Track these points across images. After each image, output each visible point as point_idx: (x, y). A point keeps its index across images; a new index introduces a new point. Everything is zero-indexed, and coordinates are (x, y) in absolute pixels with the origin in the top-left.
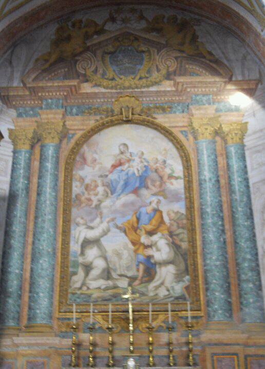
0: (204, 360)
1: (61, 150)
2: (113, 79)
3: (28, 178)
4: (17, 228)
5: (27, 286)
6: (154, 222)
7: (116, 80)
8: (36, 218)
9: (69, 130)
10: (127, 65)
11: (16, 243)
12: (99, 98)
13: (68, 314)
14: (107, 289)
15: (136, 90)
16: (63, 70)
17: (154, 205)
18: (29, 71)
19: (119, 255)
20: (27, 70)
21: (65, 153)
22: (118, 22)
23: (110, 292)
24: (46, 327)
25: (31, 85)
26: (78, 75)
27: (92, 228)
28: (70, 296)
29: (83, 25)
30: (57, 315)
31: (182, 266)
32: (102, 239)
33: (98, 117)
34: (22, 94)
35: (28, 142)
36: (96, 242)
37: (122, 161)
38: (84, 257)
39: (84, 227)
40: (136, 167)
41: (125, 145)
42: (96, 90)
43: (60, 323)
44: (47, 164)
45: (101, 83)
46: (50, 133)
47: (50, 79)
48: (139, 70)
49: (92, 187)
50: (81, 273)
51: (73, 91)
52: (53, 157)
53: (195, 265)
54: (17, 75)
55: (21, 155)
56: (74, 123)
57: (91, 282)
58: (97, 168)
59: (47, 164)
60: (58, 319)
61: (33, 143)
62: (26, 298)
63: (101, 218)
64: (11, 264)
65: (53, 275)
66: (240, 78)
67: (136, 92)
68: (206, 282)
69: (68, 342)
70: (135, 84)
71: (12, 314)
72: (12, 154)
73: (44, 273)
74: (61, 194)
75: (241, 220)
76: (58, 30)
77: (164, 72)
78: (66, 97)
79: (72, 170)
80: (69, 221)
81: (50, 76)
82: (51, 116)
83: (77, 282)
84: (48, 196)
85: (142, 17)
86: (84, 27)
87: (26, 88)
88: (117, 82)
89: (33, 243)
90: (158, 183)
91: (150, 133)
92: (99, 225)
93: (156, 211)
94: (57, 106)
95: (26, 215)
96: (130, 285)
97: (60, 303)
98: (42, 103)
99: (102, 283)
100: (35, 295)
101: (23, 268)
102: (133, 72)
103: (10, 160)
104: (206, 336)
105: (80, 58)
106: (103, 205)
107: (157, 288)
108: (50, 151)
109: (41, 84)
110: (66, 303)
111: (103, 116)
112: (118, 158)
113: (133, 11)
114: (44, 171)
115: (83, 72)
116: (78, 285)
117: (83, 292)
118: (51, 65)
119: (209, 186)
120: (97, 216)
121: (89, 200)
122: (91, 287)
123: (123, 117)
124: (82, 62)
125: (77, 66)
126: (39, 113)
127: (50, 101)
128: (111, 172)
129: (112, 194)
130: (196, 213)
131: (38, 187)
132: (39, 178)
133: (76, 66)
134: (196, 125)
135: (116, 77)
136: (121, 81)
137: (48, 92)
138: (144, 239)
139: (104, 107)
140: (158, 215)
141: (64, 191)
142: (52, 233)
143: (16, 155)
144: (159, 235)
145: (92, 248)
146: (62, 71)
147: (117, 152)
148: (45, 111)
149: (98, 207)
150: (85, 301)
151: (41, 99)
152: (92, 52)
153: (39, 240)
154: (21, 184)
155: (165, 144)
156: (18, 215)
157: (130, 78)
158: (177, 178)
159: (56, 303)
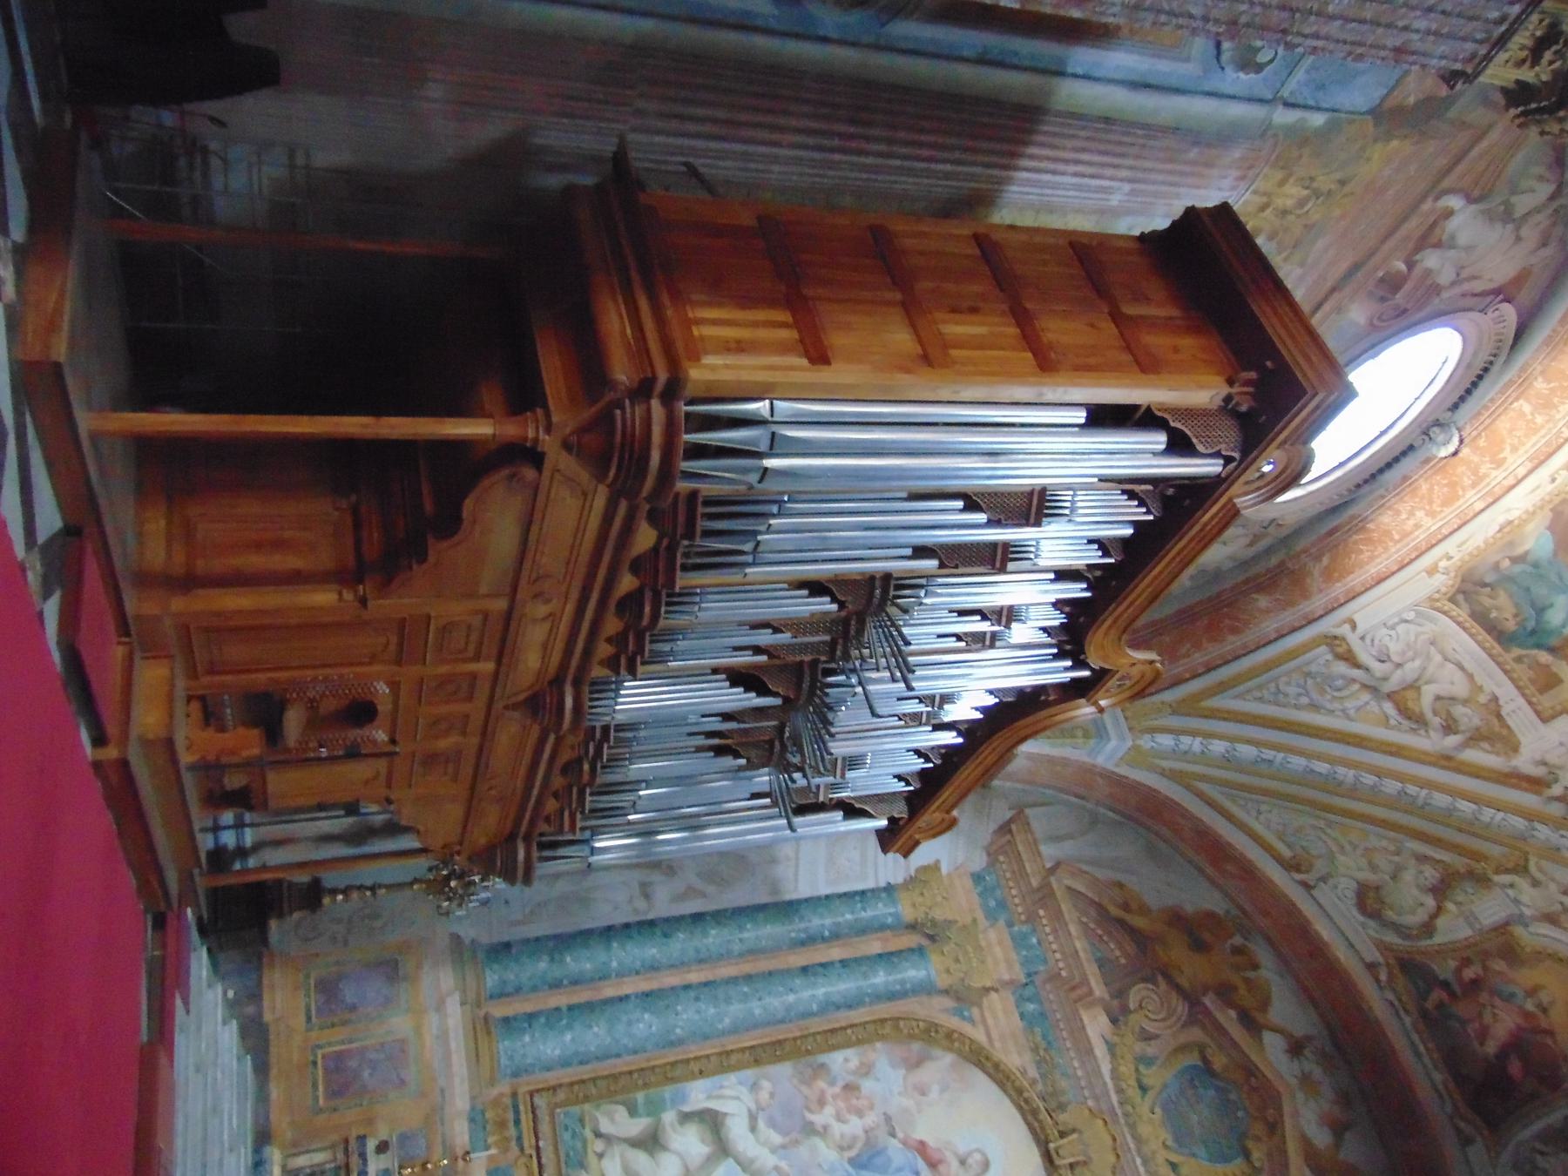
1: (924, 998)
2: (1143, 1089)
3: (836, 936)
4: (714, 938)
5: (582, 996)
7: (1143, 1097)
8: (748, 978)
9: (980, 1006)
10: (1195, 1118)
11: (681, 944)
12: (1083, 1063)
13: (531, 1116)
15: (1139, 1161)
16: (1118, 953)
18: (1086, 873)
20: (1085, 867)
24: (492, 1068)
25: (1055, 885)
26: (1120, 994)
28: (576, 1109)
29: (1251, 974)
30: (523, 1090)
32: (731, 1161)
33: (1033, 1073)
34: (1029, 870)
35: (921, 917)
36: (722, 1148)
37: (941, 1168)
38: (676, 1123)
39: (753, 1107)
41: (986, 1165)
42: (1100, 1051)
43: (508, 1101)
44: (881, 973)
45: (1122, 1058)
46: (957, 960)
48: (1194, 1155)
49: (854, 1102)
50: (636, 1126)
51: (1076, 991)
52: (903, 982)
54: (1066, 849)
55: (885, 905)
56: (1000, 1014)
57: (618, 1159)
58: (907, 1102)
59: (881, 973)
60: (514, 1095)
61: (923, 925)
63: (784, 1147)
64: (629, 946)
65: (618, 1056)
67: (1134, 1161)
69: (460, 1133)
70: (1154, 1153)
71: (512, 977)
72: (882, 884)
73: (621, 1028)
74: (816, 1025)
76: (1210, 915)
78: (1054, 977)
79: (883, 1038)
80: (757, 1062)
81: (1092, 925)
82: (998, 950)
83: (612, 1120)
84: (806, 994)
85: (1339, 1129)
86: (1247, 981)
87: (1045, 878)
88: (1138, 1100)
89: (687, 987)
92: (764, 1144)
94: (1026, 962)
97: (554, 1089)
98: (1023, 923)
100: (564, 1022)
101: (623, 976)
102: (1182, 1138)
103: (869, 884)
105: (1163, 985)
106: (818, 1142)
109: (1065, 907)
110: (557, 1105)
111: (1040, 1087)
112: (949, 1155)
113: (1344, 1099)
114: (864, 969)
115: (1132, 1006)
116: (605, 1126)
117: (589, 1145)
118: (1121, 922)
120: (784, 1133)
121: (822, 1102)
122: (606, 1163)
123: (1056, 1140)
124: (1155, 997)
125: (1142, 985)
126: (996, 920)
127: (1034, 940)
128: (905, 1143)
129: (852, 1161)
131: (822, 965)
132: (841, 961)
133: (1145, 980)
135: (1151, 1095)
136: (1144, 1110)
137: (1055, 931)
139: (1064, 1084)
141: (825, 1032)
142: (720, 1027)
143: (884, 895)
145: (703, 1141)
146: (1113, 950)
147: (962, 1149)
148: (1007, 937)
149: (810, 1130)
150: (568, 1155)
151: (1031, 918)
152: (1190, 1015)
153: (697, 999)
154: (820, 922)
156: (746, 935)
157: (1166, 1136)
159: (552, 1077)
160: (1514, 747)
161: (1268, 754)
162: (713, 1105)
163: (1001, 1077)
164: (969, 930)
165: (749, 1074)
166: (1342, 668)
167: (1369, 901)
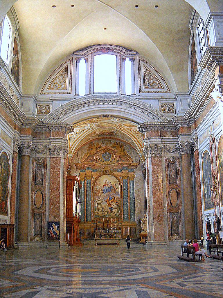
19: (105, 207)
22: (105, 144)
23: (103, 215)
36: (100, 204)
40: (109, 186)
42: (99, 165)
75: (132, 199)
90: (114, 190)
91: (113, 177)
95: (84, 197)
99: (102, 213)
102: (109, 160)
113: (108, 141)
121: (98, 194)
144: (114, 202)
149: (100, 196)
160: (86, 129)
163: (100, 176)
166: (72, 135)
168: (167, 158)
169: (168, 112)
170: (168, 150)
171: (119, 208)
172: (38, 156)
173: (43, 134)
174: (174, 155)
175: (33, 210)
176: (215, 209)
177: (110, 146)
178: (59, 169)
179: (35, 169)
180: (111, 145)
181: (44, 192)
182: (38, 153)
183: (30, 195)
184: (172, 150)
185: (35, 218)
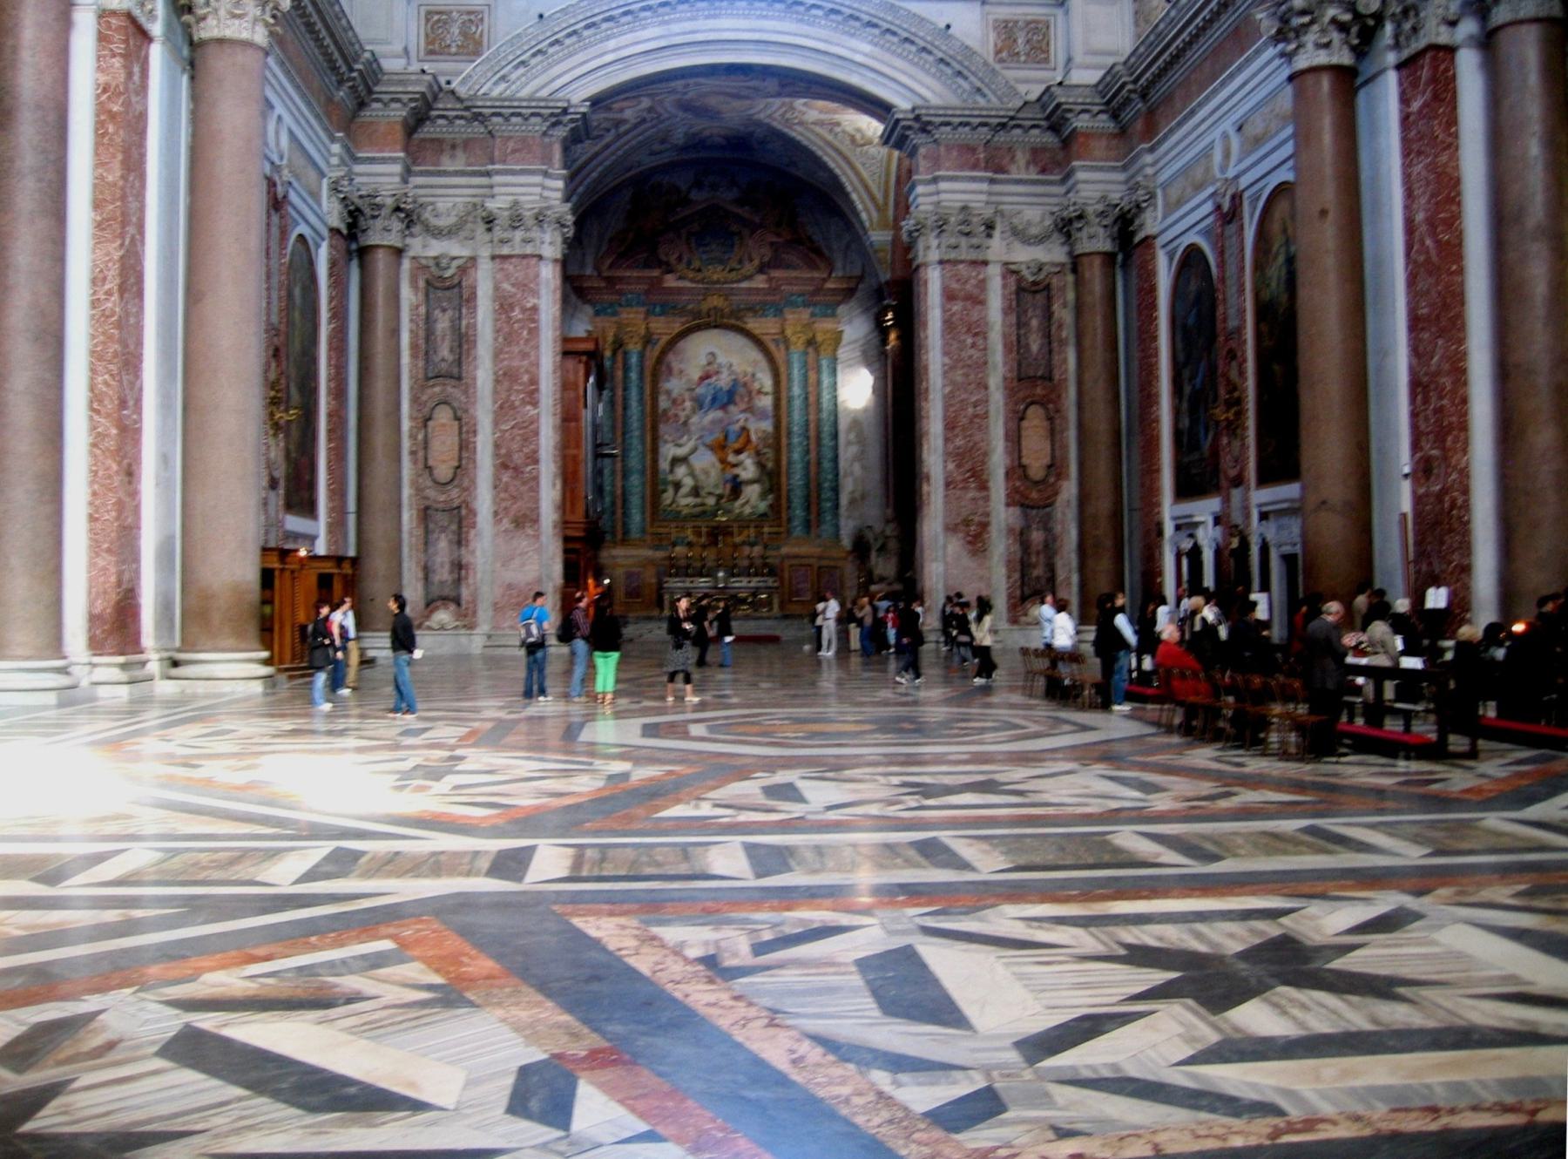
0: (782, 571)
2: (699, 270)
5: (619, 503)
6: (742, 440)
8: (624, 434)
14: (695, 506)
17: (741, 423)
19: (707, 473)
21: (649, 363)
26: (660, 264)
27: (680, 446)
31: (767, 485)
40: (724, 381)
41: (713, 354)
42: (681, 284)
47: (629, 267)
50: (671, 491)
53: (779, 484)
54: (590, 260)
58: (684, 380)
60: (653, 534)
62: (619, 512)
66: (840, 274)
68: (789, 501)
69: (660, 554)
75: (827, 441)
77: (756, 262)
78: (647, 292)
82: (632, 316)
91: (739, 341)
93: (744, 429)
94: (638, 304)
96: (718, 503)
99: (690, 500)
104: (785, 550)
107: (743, 505)
108: (634, 360)
116: (668, 502)
119: (797, 403)
121: (676, 415)
130: (784, 432)
134: (789, 332)
138: (732, 458)
139: (690, 307)
140: (744, 435)
149: (685, 423)
151: (620, 293)
155: (754, 354)
157: (720, 268)
158: (766, 394)
161: (586, 183)
162: (670, 458)
163: (683, 334)
164: (620, 326)
165: (661, 444)
167: (652, 153)
168: (1013, 267)
169: (1023, 58)
170: (1019, 234)
171: (771, 478)
172: (436, 248)
173: (454, 147)
174: (1039, 254)
175: (418, 490)
176: (1227, 500)
177: (726, 196)
178: (535, 309)
179: (422, 310)
180: (733, 194)
181: (466, 411)
182: (438, 233)
183: (406, 425)
184: (1034, 231)
185: (431, 526)
